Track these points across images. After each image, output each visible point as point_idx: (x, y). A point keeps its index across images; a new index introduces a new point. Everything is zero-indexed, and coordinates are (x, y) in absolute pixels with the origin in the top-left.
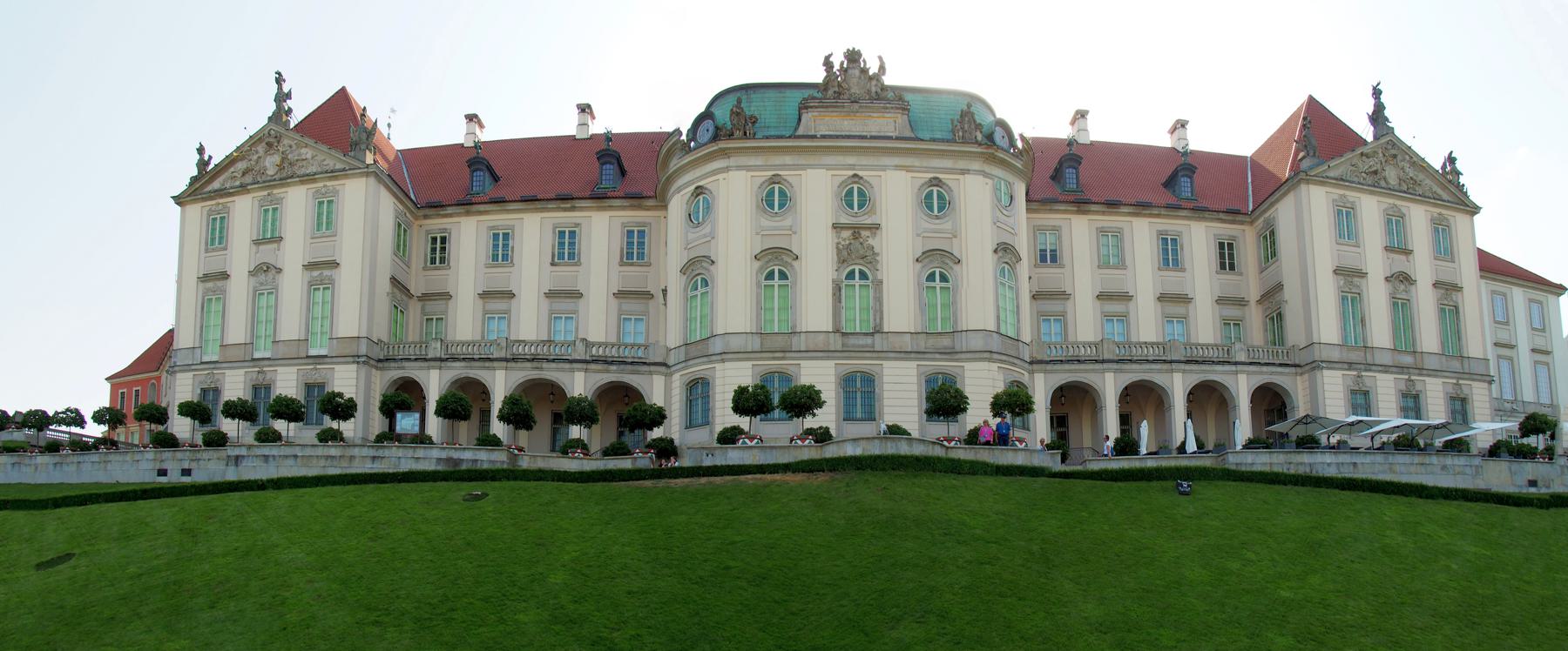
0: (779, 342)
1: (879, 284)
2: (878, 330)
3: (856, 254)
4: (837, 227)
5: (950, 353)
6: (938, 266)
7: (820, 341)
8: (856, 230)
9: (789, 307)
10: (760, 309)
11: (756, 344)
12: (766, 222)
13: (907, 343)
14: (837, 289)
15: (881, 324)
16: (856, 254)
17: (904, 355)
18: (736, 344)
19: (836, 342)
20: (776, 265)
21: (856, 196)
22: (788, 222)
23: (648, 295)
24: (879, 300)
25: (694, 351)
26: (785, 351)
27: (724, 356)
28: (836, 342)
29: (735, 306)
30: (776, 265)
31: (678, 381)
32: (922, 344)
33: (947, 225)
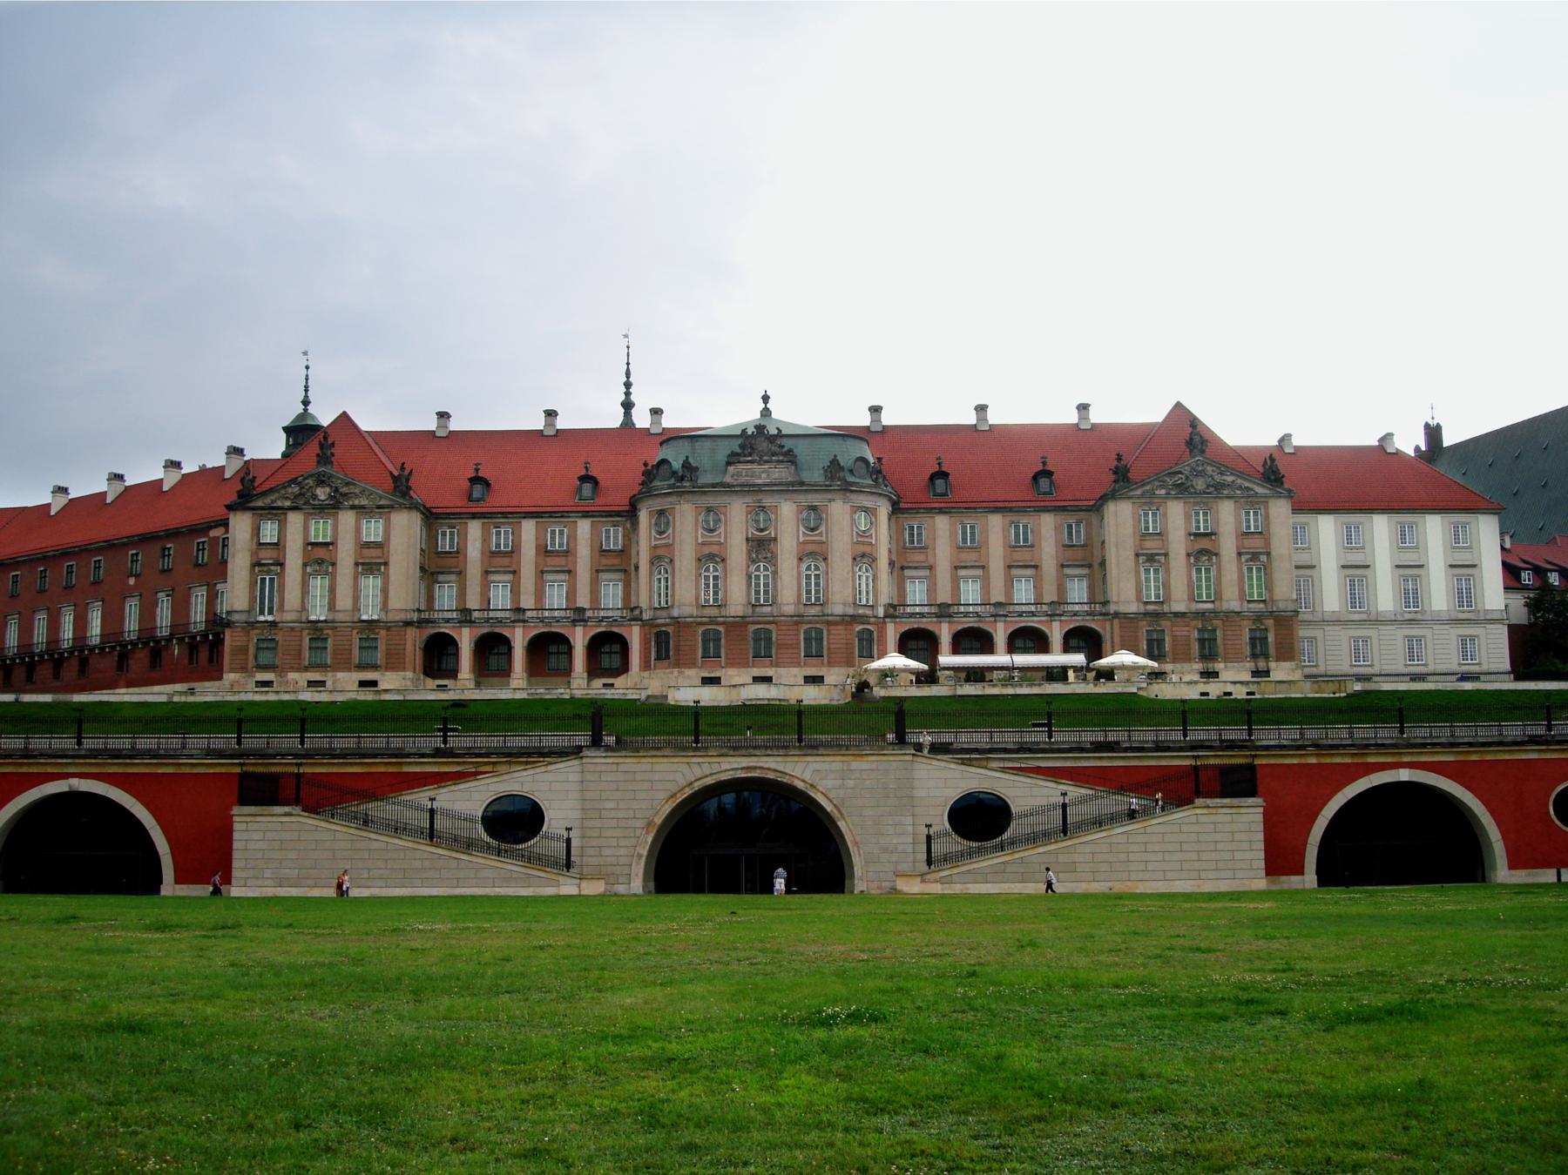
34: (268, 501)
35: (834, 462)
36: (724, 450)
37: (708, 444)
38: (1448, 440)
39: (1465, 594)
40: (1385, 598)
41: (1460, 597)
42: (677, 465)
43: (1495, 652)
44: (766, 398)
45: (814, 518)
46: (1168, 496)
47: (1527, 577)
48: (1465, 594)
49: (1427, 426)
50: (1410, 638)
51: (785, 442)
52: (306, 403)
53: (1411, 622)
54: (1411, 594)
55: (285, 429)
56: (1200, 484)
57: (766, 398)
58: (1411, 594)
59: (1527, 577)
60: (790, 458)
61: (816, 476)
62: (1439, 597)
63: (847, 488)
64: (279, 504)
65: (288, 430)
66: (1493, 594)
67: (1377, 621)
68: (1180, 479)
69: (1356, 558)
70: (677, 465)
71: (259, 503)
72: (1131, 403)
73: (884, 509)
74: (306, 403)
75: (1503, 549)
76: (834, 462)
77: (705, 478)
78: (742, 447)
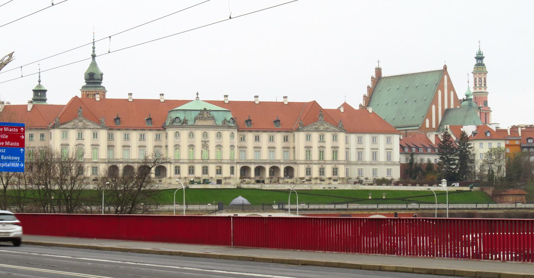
0: (192, 161)
1: (209, 151)
2: (209, 159)
3: (205, 145)
4: (202, 141)
5: (221, 163)
6: (219, 146)
7: (199, 161)
8: (205, 142)
9: (193, 154)
10: (189, 155)
11: (188, 161)
12: (190, 140)
13: (213, 161)
14: (202, 151)
15: (209, 156)
16: (205, 145)
17: (213, 163)
18: (185, 161)
19: (201, 161)
20: (192, 146)
21: (205, 135)
22: (193, 140)
23: (161, 147)
24: (209, 154)
25: (176, 161)
26: (193, 163)
27: (183, 163)
28: (201, 161)
29: (184, 154)
30: (192, 146)
31: (173, 166)
32: (216, 161)
33: (220, 140)
34: (64, 126)
35: (225, 120)
36: (194, 115)
37: (189, 112)
38: (384, 75)
39: (389, 156)
40: (367, 157)
41: (388, 158)
42: (182, 118)
43: (396, 174)
44: (197, 94)
45: (219, 136)
46: (313, 131)
47: (407, 150)
48: (389, 156)
49: (376, 69)
50: (373, 169)
51: (212, 112)
52: (39, 81)
53: (375, 164)
54: (374, 155)
55: (34, 91)
56: (322, 128)
57: (197, 94)
58: (374, 155)
59: (407, 150)
60: (213, 118)
61: (220, 123)
62: (382, 157)
63: (230, 127)
64: (68, 127)
65: (35, 91)
66: (397, 157)
67: (366, 164)
68: (317, 126)
69: (360, 146)
70: (182, 118)
71: (62, 127)
72: (299, 95)
73: (236, 133)
74: (39, 81)
75: (400, 139)
76: (225, 120)
77: (190, 123)
78: (200, 114)
